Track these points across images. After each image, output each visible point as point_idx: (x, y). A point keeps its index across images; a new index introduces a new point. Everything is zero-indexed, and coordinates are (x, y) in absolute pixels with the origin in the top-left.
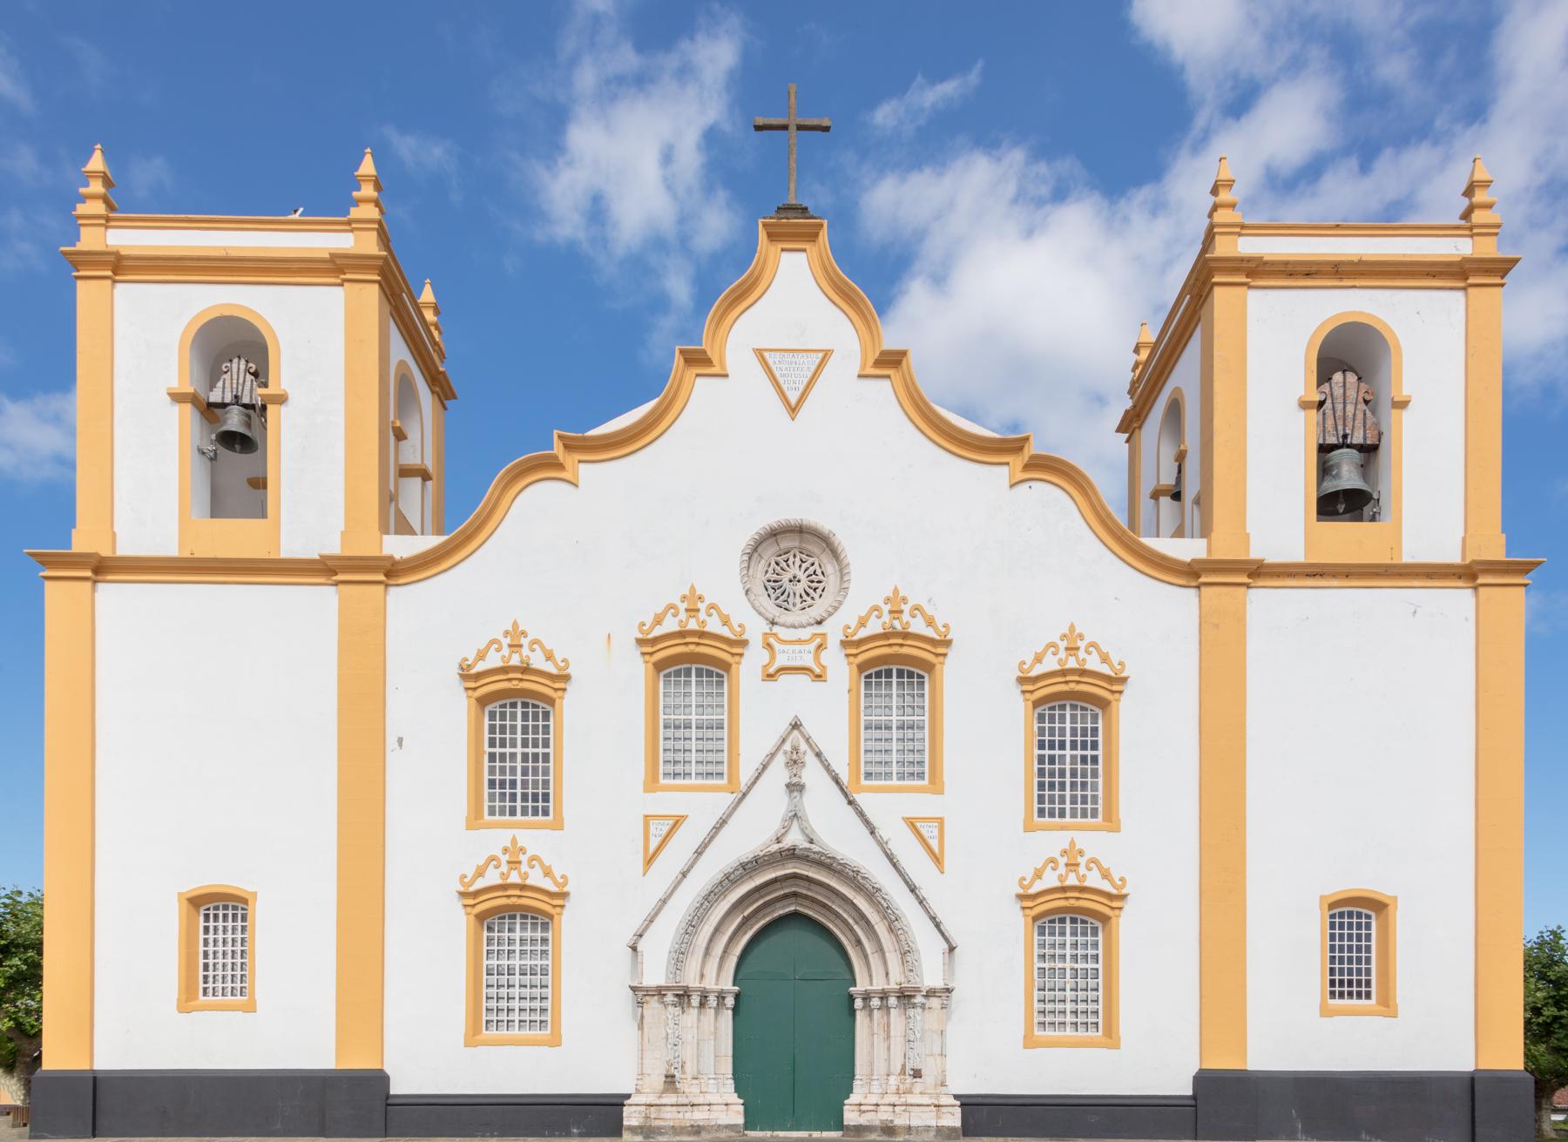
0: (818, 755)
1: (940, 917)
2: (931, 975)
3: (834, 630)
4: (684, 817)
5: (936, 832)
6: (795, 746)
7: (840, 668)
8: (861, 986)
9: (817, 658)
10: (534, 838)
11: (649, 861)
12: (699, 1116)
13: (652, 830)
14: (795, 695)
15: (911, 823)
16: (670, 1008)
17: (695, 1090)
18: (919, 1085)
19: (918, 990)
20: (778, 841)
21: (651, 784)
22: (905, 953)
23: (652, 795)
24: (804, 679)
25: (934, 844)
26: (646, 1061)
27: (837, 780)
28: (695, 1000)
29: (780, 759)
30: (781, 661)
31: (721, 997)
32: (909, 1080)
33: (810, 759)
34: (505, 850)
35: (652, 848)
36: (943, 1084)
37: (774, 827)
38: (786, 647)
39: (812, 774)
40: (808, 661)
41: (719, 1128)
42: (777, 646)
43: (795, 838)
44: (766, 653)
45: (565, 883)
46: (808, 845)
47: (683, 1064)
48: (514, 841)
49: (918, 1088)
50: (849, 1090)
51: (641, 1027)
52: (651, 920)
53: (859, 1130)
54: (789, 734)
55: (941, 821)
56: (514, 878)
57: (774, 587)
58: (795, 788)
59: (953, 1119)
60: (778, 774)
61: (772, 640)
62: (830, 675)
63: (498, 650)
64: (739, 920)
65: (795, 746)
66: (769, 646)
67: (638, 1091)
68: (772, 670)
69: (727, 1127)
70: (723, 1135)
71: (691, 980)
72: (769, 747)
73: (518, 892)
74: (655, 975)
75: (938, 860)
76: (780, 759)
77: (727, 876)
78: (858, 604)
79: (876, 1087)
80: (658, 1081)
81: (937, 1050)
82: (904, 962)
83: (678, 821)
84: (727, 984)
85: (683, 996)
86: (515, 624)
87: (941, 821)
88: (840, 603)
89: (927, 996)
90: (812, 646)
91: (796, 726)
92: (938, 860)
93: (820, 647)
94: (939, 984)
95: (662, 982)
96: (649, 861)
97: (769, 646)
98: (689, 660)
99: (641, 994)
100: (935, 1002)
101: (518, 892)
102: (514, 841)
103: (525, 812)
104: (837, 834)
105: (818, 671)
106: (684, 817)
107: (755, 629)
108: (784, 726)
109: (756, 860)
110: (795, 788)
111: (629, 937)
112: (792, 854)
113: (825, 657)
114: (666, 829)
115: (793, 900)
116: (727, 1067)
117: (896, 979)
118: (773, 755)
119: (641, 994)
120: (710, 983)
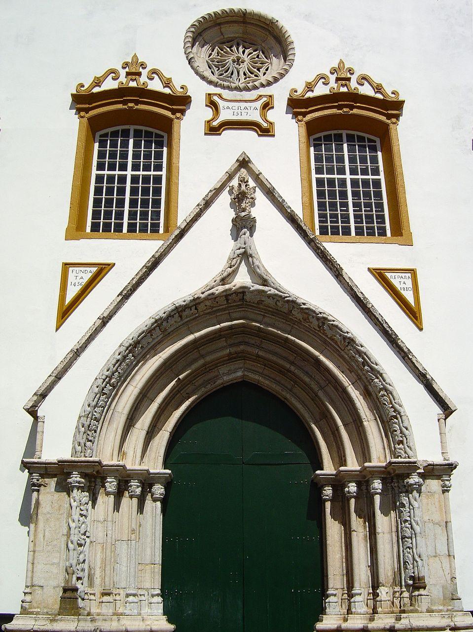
1: (433, 373)
2: (425, 449)
3: (280, 93)
4: (110, 266)
5: (409, 283)
6: (243, 186)
8: (329, 468)
9: (264, 116)
15: (380, 275)
16: (76, 493)
18: (425, 599)
19: (412, 467)
20: (223, 281)
21: (76, 230)
22: (390, 420)
25: (409, 296)
26: (39, 567)
27: (292, 219)
28: (111, 484)
30: (226, 115)
31: (148, 481)
33: (260, 197)
35: (69, 299)
36: (454, 598)
38: (230, 104)
39: (262, 210)
42: (221, 104)
43: (243, 279)
46: (261, 288)
49: (424, 603)
50: (320, 611)
54: (237, 170)
55: (413, 272)
57: (218, 65)
58: (243, 224)
60: (222, 212)
61: (216, 98)
62: (277, 130)
65: (243, 186)
67: (24, 611)
68: (215, 124)
71: (106, 453)
72: (214, 182)
74: (57, 447)
75: (413, 313)
78: (308, 68)
79: (361, 603)
80: (52, 596)
81: (442, 549)
83: (102, 270)
84: (155, 464)
85: (94, 477)
87: (413, 272)
88: (287, 71)
89: (423, 476)
90: (259, 104)
91: (244, 163)
92: (413, 313)
93: (267, 106)
94: (437, 459)
95: (67, 456)
96: (65, 312)
97: (213, 105)
99: (39, 472)
100: (434, 485)
105: (265, 125)
106: (110, 266)
107: (198, 90)
108: (230, 163)
109: (196, 303)
111: (27, 397)
113: (271, 115)
115: (239, 364)
116: (153, 580)
117: (379, 457)
118: (217, 192)
120: (132, 463)
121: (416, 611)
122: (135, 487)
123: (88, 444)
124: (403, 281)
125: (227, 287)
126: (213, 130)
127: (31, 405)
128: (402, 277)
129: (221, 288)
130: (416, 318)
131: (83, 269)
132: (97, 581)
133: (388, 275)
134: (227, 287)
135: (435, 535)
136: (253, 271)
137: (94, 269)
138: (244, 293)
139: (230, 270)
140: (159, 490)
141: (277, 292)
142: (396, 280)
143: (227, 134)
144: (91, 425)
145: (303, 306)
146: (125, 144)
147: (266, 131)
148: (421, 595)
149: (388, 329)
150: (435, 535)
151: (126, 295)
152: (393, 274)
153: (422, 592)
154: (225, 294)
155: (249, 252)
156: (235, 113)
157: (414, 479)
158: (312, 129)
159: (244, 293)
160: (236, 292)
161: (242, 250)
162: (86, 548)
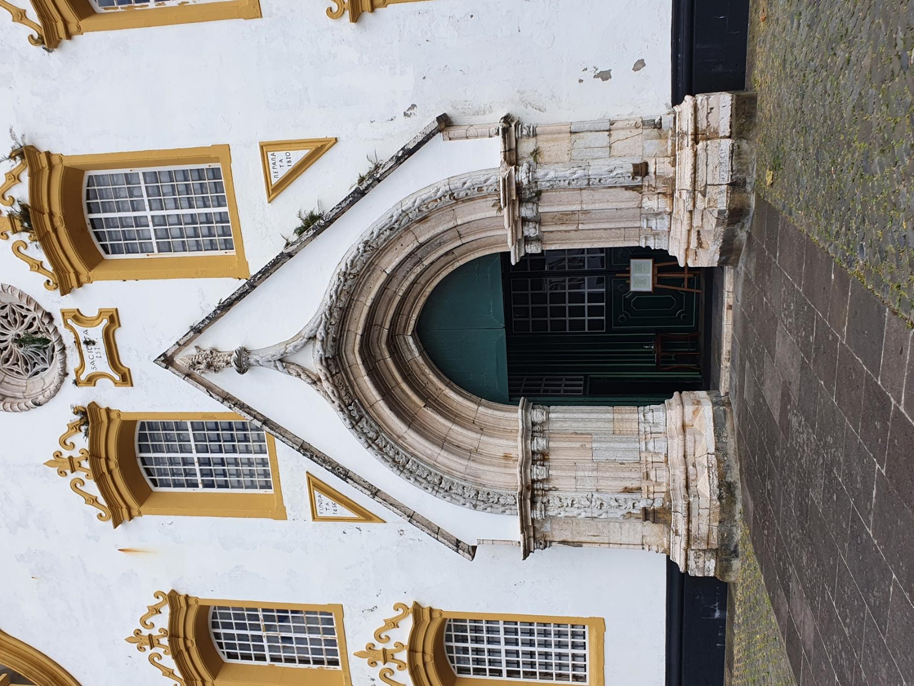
0: (197, 330)
5: (280, 155)
7: (98, 294)
10: (358, 634)
11: (367, 516)
12: (705, 486)
13: (329, 514)
14: (139, 346)
15: (275, 190)
17: (662, 475)
18: (660, 166)
20: (316, 381)
22: (454, 198)
23: (288, 511)
24: (121, 337)
25: (298, 155)
29: (211, 378)
30: (103, 365)
31: (531, 431)
32: (651, 180)
33: (207, 341)
34: (373, 663)
37: (303, 386)
40: (96, 333)
41: (719, 449)
43: (312, 359)
44: (100, 382)
45: (404, 606)
46: (318, 345)
47: (627, 490)
48: (360, 655)
51: (579, 544)
52: (436, 532)
53: (728, 251)
55: (265, 148)
56: (403, 656)
59: (720, 106)
61: (83, 377)
62: (109, 305)
63: (160, 657)
64: (429, 412)
66: (91, 380)
68: (117, 378)
69: (718, 435)
70: (731, 443)
73: (419, 656)
75: (318, 150)
76: (211, 378)
77: (371, 442)
82: (469, 199)
83: (315, 484)
86: (129, 640)
87: (265, 148)
91: (167, 361)
93: (78, 317)
96: (367, 516)
97: (91, 380)
98: (129, 465)
101: (419, 656)
102: (360, 655)
103: (331, 631)
104: (298, 303)
105: (105, 322)
107: (75, 396)
108: (169, 374)
109: (344, 407)
110: (243, 362)
111: (461, 559)
112: (335, 362)
113: (90, 311)
114: (325, 499)
119: (534, 539)
121: (674, 180)
122: (540, 444)
123: (502, 501)
124: (278, 163)
125: (323, 378)
126: (126, 378)
127: (467, 555)
128: (274, 164)
129: (326, 384)
130: (323, 146)
131: (318, 504)
132: (636, 484)
133: (274, 181)
134: (323, 378)
135: (586, 148)
136: (297, 350)
137: (317, 493)
138: (326, 359)
139: (303, 376)
140: (537, 415)
141: (322, 327)
142: (279, 172)
143: (126, 359)
144: (482, 499)
145: (334, 297)
146: (158, 461)
147: (114, 319)
148: (655, 173)
149: (348, 202)
150: (586, 148)
151: (346, 475)
152: (273, 175)
153: (652, 169)
154: (330, 379)
155: (279, 357)
156: (99, 355)
157: (522, 176)
158: (92, 260)
159: (326, 359)
160: (328, 367)
161: (278, 364)
162: (605, 497)
